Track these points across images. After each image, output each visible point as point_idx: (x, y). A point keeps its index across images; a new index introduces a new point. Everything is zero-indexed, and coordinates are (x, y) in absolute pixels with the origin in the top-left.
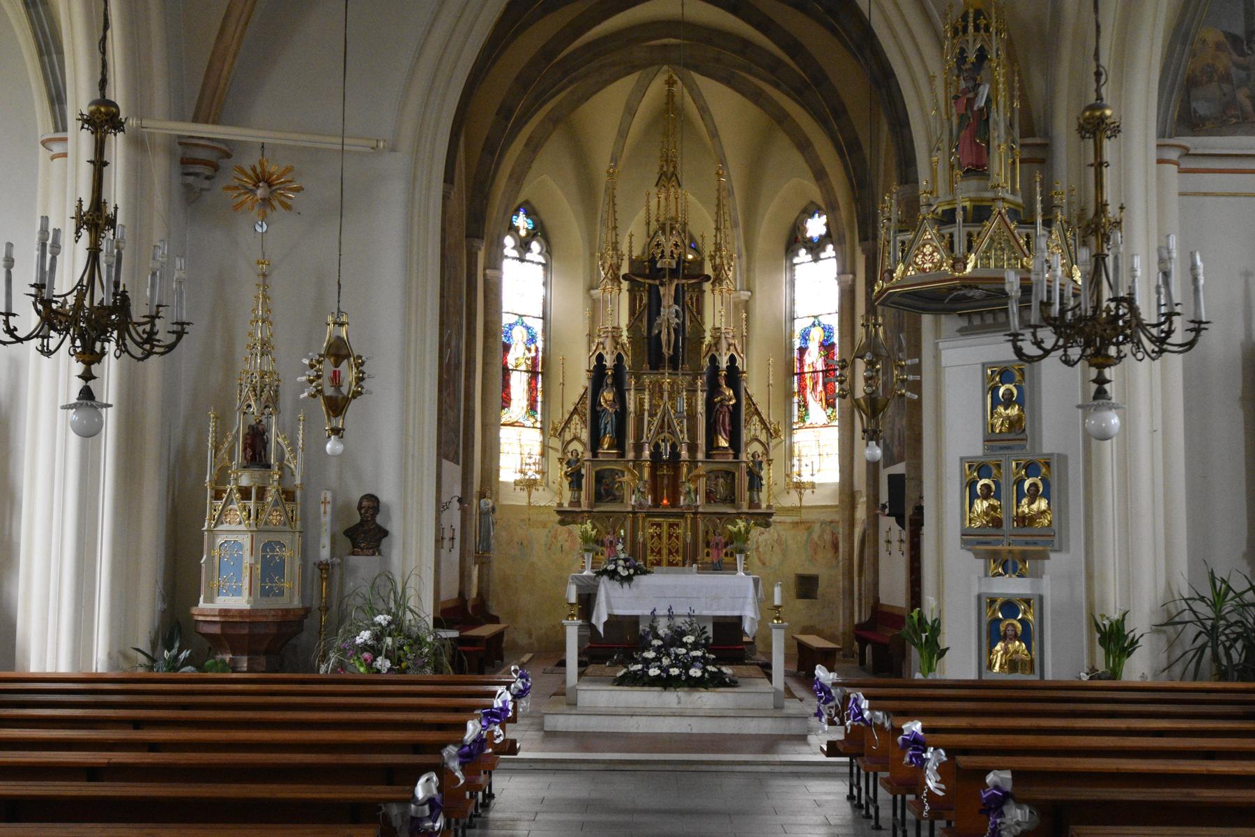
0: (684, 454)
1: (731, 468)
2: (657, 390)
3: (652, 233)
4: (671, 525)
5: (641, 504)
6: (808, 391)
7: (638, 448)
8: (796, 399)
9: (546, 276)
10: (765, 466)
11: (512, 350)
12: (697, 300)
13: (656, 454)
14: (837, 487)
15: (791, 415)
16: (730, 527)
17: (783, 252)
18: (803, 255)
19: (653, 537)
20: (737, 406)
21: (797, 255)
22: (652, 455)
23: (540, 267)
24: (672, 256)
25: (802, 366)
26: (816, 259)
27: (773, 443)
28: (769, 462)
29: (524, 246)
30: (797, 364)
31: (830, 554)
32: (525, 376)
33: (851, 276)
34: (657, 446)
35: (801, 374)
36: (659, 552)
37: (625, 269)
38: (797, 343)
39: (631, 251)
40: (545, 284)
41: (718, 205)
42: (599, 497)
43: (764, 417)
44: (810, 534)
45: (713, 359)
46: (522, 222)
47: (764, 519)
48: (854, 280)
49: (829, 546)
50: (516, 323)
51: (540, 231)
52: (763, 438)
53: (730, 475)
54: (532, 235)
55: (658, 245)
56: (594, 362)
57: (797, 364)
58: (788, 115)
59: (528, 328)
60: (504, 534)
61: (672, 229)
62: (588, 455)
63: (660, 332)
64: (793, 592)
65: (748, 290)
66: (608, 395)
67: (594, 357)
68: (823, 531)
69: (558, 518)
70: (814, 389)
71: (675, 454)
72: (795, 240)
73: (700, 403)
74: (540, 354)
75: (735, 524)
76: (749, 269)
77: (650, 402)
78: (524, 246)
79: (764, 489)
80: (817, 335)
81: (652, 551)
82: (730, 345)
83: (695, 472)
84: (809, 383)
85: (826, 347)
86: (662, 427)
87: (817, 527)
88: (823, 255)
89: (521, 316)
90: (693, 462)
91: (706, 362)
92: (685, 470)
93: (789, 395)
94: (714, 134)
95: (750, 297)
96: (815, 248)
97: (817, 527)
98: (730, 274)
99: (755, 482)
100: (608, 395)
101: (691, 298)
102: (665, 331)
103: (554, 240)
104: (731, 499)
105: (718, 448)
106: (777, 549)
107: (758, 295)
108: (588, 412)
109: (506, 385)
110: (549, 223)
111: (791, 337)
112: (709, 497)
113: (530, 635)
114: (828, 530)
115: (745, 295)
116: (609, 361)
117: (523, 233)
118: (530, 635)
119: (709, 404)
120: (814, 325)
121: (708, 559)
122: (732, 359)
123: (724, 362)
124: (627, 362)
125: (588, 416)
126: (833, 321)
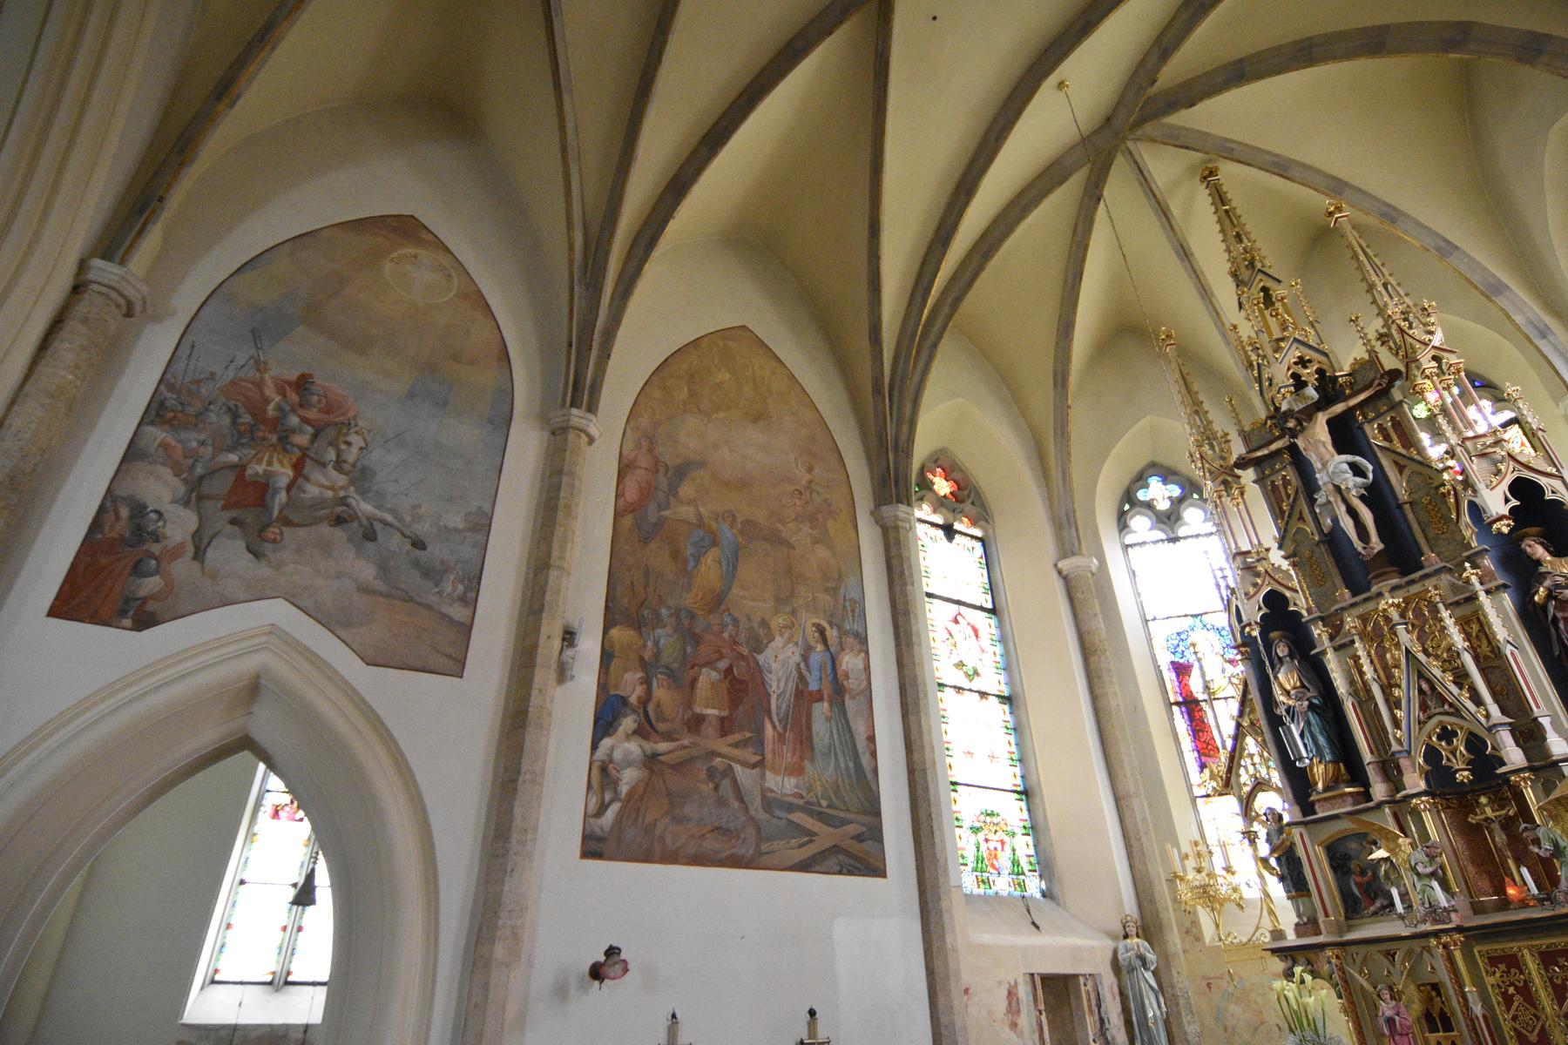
0: (1514, 756)
2: (1378, 636)
7: (1391, 770)
12: (1397, 425)
19: (1508, 1000)
23: (1215, 538)
29: (1169, 520)
34: (1432, 755)
37: (1238, 449)
42: (1353, 908)
45: (1476, 511)
46: (1159, 492)
54: (1178, 503)
60: (1235, 1009)
63: (1335, 520)
69: (1278, 965)
71: (1484, 761)
78: (1169, 520)
82: (1495, 463)
86: (1424, 707)
89: (1195, 616)
91: (1468, 530)
92: (1529, 794)
94: (1337, 187)
100: (1286, 679)
101: (1382, 429)
108: (1263, 723)
116: (1253, 612)
123: (1496, 502)
124: (1301, 602)
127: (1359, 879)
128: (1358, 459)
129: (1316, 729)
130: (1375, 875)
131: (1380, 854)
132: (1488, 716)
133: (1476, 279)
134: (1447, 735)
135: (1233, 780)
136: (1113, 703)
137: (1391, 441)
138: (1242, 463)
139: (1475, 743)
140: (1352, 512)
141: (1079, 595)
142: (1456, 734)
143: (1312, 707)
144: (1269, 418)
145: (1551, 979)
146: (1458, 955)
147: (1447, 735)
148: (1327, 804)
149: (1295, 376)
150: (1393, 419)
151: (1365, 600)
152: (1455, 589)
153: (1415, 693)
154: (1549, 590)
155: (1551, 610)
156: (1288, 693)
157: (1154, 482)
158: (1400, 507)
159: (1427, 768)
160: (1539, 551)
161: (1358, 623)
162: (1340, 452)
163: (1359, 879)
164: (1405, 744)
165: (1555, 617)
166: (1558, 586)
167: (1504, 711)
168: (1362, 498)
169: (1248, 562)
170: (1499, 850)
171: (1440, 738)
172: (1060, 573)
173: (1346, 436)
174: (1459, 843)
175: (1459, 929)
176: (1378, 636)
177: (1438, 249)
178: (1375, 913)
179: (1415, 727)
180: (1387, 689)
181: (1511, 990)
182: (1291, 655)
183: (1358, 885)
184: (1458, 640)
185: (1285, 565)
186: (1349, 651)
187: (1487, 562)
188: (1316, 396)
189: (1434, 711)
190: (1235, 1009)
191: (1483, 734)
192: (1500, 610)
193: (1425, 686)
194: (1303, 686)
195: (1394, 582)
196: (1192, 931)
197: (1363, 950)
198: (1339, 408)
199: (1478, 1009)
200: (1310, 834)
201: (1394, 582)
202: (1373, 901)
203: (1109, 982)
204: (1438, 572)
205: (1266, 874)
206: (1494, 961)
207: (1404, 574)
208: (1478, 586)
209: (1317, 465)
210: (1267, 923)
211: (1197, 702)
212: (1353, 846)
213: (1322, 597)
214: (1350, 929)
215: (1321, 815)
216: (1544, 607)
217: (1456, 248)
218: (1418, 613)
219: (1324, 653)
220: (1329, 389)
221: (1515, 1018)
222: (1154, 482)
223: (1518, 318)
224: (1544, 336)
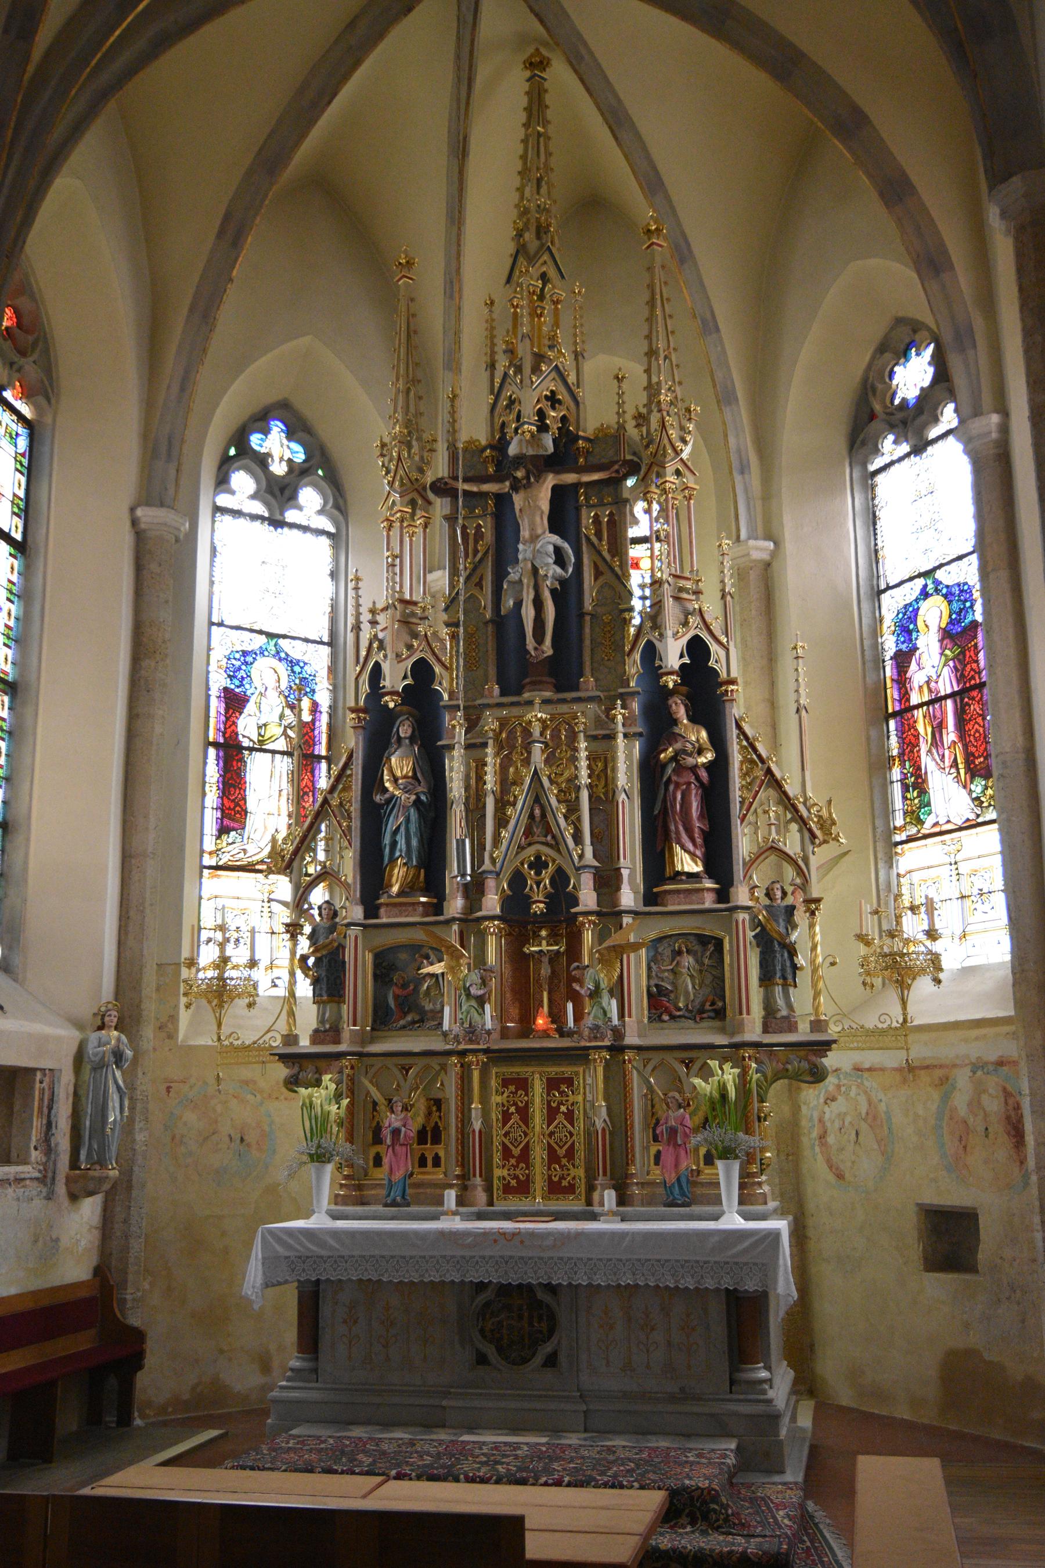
0: (588, 898)
1: (710, 929)
2: (514, 743)
3: (498, 380)
4: (552, 1084)
5: (472, 1032)
6: (924, 748)
8: (896, 773)
9: (336, 559)
10: (800, 916)
11: (250, 707)
13: (516, 901)
14: (1006, 973)
15: (887, 812)
16: (697, 1081)
17: (844, 452)
18: (890, 447)
19: (506, 1117)
20: (719, 767)
21: (877, 451)
22: (507, 902)
23: (325, 542)
24: (543, 428)
25: (904, 695)
26: (918, 450)
27: (819, 856)
28: (812, 904)
29: (279, 493)
30: (893, 693)
31: (1003, 1150)
32: (284, 765)
33: (995, 418)
34: (517, 880)
35: (906, 711)
36: (525, 1156)
38: (890, 644)
39: (453, 431)
40: (334, 575)
41: (651, 303)
42: (382, 1019)
43: (792, 789)
44: (946, 1098)
45: (651, 653)
46: (278, 447)
47: (807, 1060)
48: (1004, 429)
49: (998, 1128)
50: (262, 652)
51: (322, 465)
52: (792, 842)
53: (710, 947)
54: (299, 473)
55: (512, 402)
56: (365, 688)
57: (893, 693)
58: (803, 55)
59: (293, 664)
60: (190, 1117)
61: (539, 358)
62: (357, 913)
63: (519, 604)
64: (915, 1251)
65: (768, 537)
66: (400, 764)
67: (365, 676)
68: (979, 1090)
69: (281, 1071)
70: (936, 742)
71: (562, 897)
72: (872, 420)
73: (622, 766)
74: (324, 719)
75: (706, 1073)
76: (768, 494)
77: (503, 769)
78: (279, 493)
79: (803, 978)
80: (934, 614)
81: (507, 1153)
82: (687, 614)
83: (615, 939)
84: (923, 728)
85: (958, 636)
86: (528, 832)
87: (963, 1079)
88: (933, 433)
89: (270, 636)
90: (609, 914)
91: (634, 667)
92: (588, 937)
93: (881, 764)
95: (774, 554)
96: (913, 423)
97: (963, 1079)
98: (686, 453)
99: (778, 960)
100: (400, 764)
101: (597, 520)
102: (528, 596)
103: (349, 481)
104: (716, 1008)
105: (678, 876)
106: (868, 1138)
107: (789, 546)
108: (355, 808)
109: (233, 782)
110: (338, 449)
111: (876, 631)
112: (659, 1002)
113: (266, 1368)
114: (992, 1083)
115: (760, 549)
116: (395, 677)
117: (279, 469)
118: (266, 1368)
119: (651, 772)
120: (925, 594)
121: (656, 1174)
122: (697, 648)
123: (673, 654)
124: (446, 684)
125: (356, 824)
126: (968, 573)
127: (398, 992)
128: (566, 545)
129: (413, 828)
130: (416, 990)
131: (438, 968)
132: (581, 857)
133: (719, 375)
134: (538, 864)
135: (295, 864)
136: (158, 729)
137: (600, 539)
138: (441, 488)
139: (560, 878)
140: (538, 604)
141: (154, 567)
142: (546, 866)
143: (418, 802)
144: (491, 446)
145: (549, 1102)
146: (476, 1074)
147: (538, 864)
148: (396, 910)
149: (541, 414)
150: (611, 514)
151: (513, 704)
152: (598, 723)
153: (524, 820)
154: (677, 753)
155: (669, 771)
156: (395, 780)
157: (277, 429)
158: (581, 615)
159: (509, 893)
160: (681, 712)
161: (496, 725)
162: (552, 531)
163: (398, 992)
164: (498, 865)
165: (669, 779)
166: (684, 751)
167: (595, 856)
168: (553, 592)
169: (407, 614)
170: (537, 981)
171: (530, 867)
172: (134, 522)
173: (562, 517)
174: (507, 971)
175: (486, 1051)
176: (514, 743)
177: (704, 321)
178: (404, 1027)
179: (514, 848)
180: (502, 804)
181: (512, 1109)
182: (412, 739)
183: (396, 997)
184: (584, 778)
185: (444, 632)
186: (477, 753)
187: (635, 706)
188: (551, 449)
189: (536, 839)
190: (190, 1117)
191: (570, 871)
192: (629, 757)
193: (537, 812)
194: (415, 777)
195: (548, 694)
196: (168, 1027)
197: (378, 1062)
198: (570, 478)
199: (477, 1125)
200: (364, 937)
201: (548, 694)
202: (405, 1014)
203: (67, 1078)
204: (590, 699)
205: (299, 973)
206: (506, 1083)
207: (559, 688)
208: (620, 728)
209: (525, 533)
210: (282, 1026)
211: (240, 748)
212: (403, 956)
213: (473, 686)
214: (373, 1040)
215: (384, 920)
216: (664, 766)
217: (718, 330)
218: (556, 735)
219: (451, 747)
220: (566, 452)
221: (506, 1134)
222: (277, 429)
223: (732, 440)
224: (742, 473)
